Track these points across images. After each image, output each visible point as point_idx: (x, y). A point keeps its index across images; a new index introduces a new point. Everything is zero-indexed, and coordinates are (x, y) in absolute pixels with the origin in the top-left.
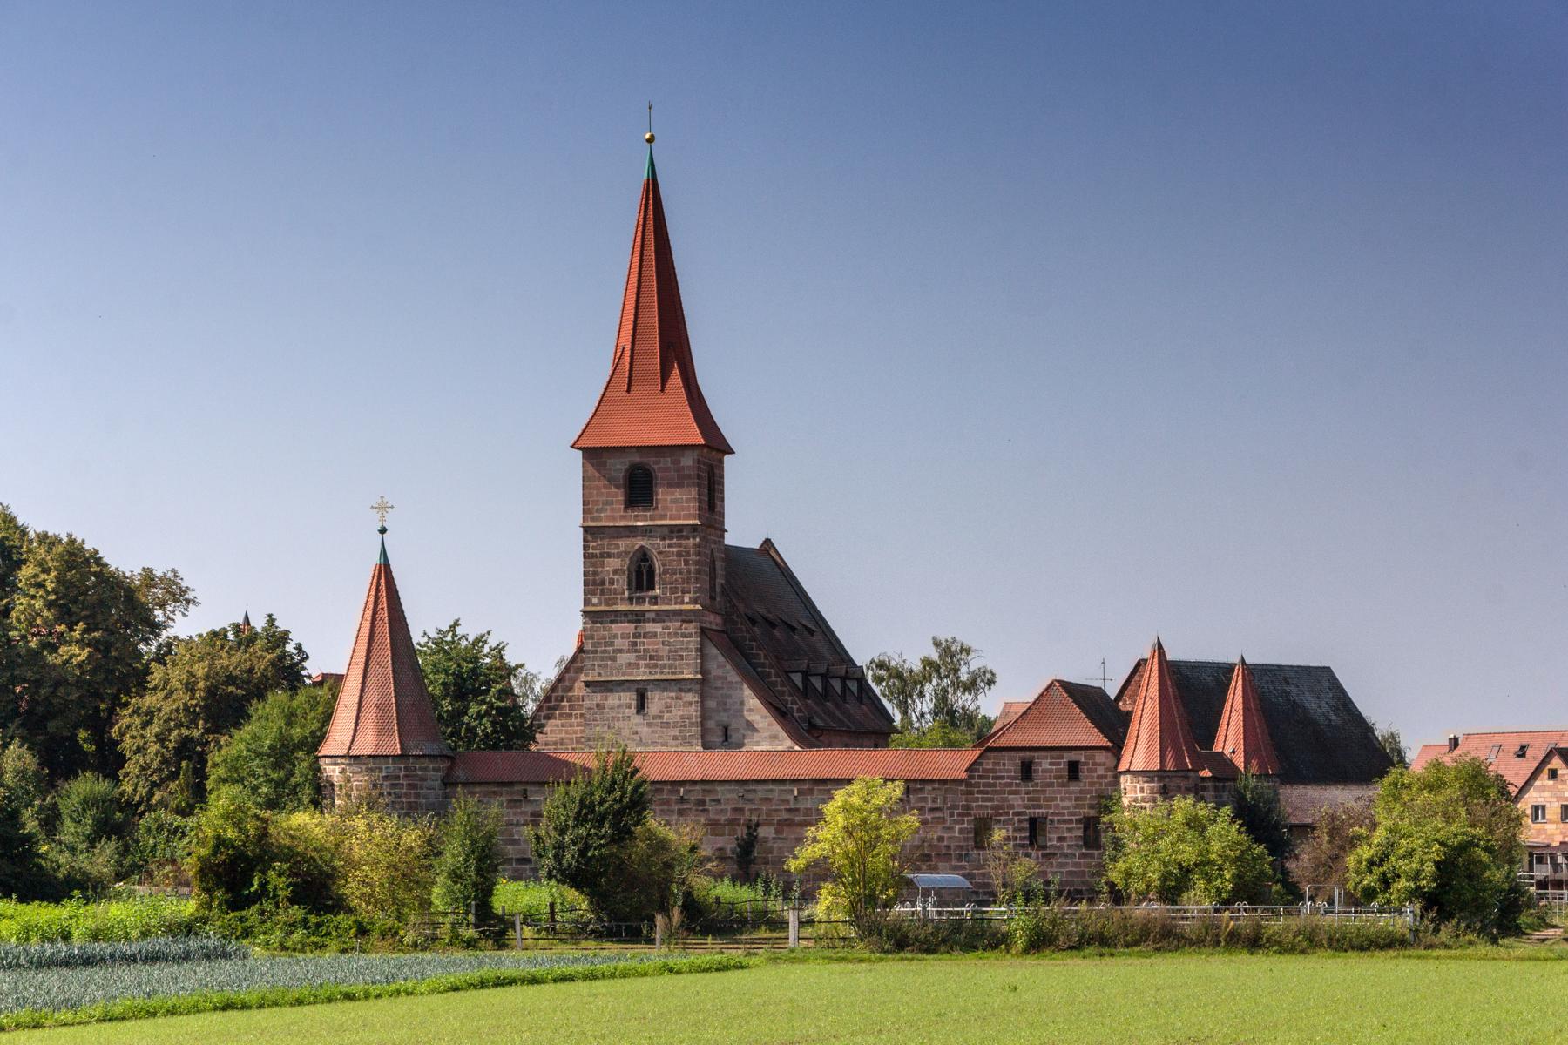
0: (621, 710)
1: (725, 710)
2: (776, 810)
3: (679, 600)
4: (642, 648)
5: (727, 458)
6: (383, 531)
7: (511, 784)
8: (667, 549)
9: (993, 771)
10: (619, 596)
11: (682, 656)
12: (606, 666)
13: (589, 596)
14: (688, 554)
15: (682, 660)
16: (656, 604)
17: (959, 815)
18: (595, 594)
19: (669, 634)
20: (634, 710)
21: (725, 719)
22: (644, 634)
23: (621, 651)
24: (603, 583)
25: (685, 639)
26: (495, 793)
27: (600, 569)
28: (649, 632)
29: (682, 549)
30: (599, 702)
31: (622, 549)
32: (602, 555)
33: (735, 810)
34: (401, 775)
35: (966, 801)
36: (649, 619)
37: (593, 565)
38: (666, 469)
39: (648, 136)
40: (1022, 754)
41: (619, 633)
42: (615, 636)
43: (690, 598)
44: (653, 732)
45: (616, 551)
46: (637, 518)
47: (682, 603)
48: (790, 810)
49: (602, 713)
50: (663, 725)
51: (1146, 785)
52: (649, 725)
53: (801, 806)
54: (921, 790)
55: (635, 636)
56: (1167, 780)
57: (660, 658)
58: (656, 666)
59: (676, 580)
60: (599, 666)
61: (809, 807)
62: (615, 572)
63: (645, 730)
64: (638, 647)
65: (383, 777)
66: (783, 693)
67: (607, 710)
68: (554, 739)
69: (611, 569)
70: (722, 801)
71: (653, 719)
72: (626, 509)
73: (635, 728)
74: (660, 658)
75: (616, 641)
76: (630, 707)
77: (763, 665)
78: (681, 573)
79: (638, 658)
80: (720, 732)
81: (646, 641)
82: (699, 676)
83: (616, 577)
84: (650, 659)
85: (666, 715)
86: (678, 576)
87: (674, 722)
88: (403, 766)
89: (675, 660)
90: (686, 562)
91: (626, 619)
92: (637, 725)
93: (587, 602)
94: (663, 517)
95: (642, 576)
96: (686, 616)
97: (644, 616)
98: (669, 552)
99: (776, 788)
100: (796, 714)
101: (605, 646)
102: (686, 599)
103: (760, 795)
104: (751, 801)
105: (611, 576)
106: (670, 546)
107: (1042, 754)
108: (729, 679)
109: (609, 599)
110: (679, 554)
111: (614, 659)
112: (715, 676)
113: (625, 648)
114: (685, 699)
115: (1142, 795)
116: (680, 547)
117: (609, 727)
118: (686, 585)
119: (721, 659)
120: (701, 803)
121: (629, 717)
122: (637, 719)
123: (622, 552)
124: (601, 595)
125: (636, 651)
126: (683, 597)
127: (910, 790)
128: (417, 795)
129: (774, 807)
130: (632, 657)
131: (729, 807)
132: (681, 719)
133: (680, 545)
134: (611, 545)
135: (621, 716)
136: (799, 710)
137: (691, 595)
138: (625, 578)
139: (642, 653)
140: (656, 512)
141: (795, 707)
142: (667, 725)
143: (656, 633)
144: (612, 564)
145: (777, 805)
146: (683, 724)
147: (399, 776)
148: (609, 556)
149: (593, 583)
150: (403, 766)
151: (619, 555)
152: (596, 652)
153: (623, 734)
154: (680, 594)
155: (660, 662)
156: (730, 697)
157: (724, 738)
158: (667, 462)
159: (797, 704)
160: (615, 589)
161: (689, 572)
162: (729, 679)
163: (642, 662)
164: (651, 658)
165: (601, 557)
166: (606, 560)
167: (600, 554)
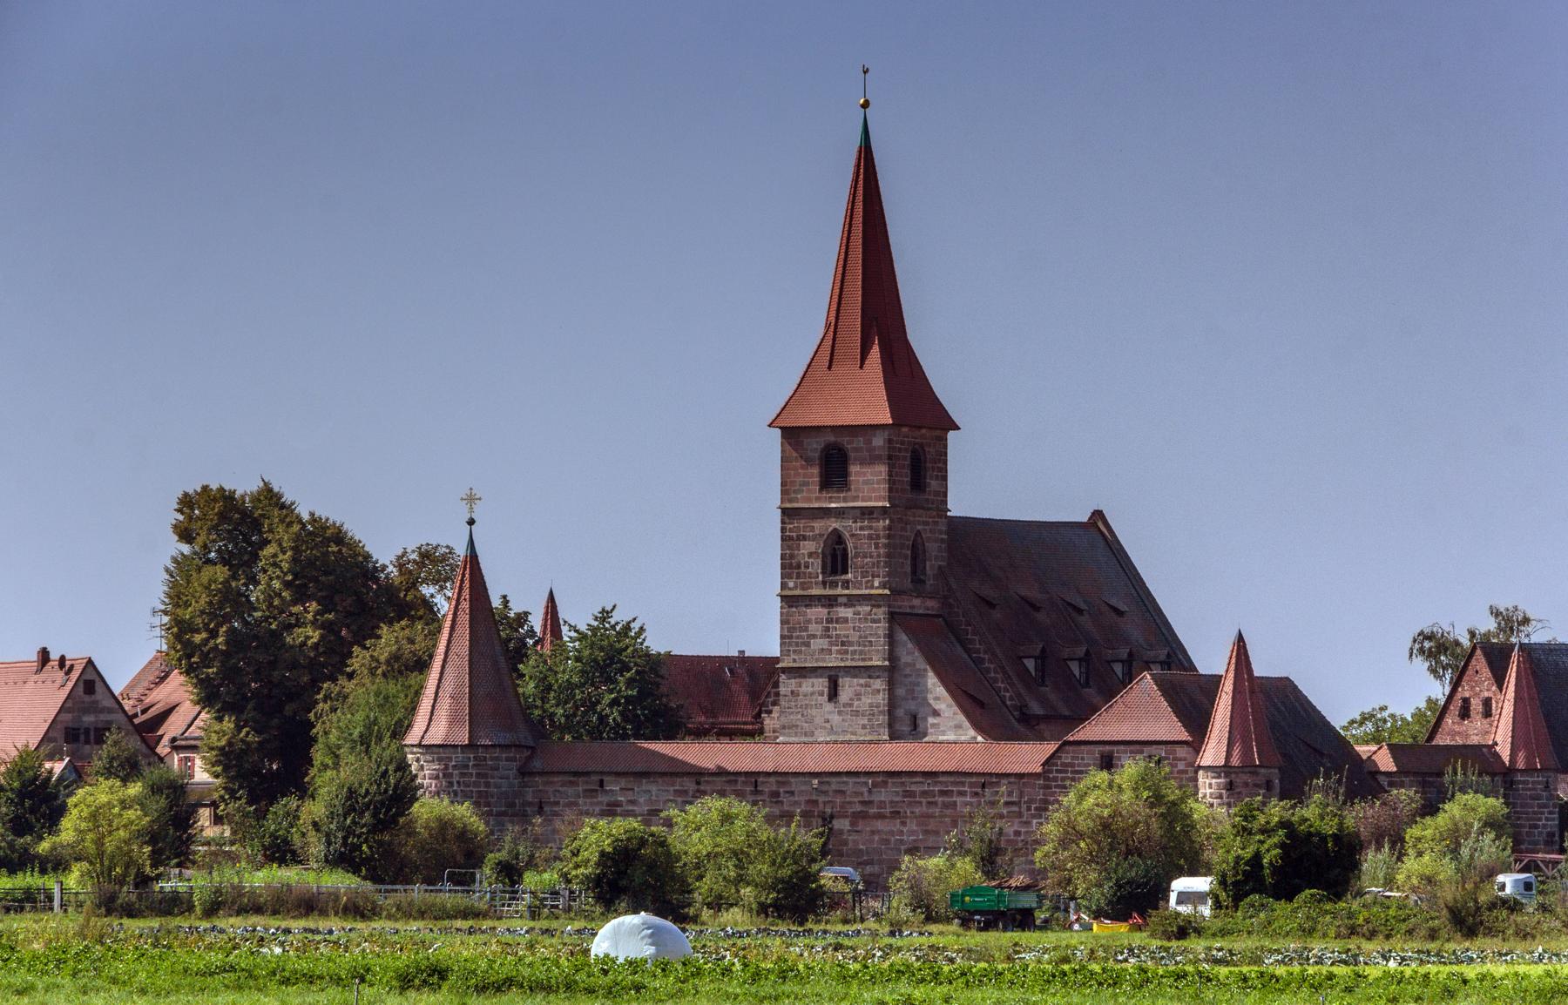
1: (913, 699)
2: (850, 803)
3: (869, 585)
5: (951, 435)
6: (471, 522)
7: (587, 774)
9: (1072, 765)
10: (813, 580)
11: (870, 642)
12: (801, 652)
13: (786, 580)
14: (878, 537)
15: (872, 646)
16: (848, 588)
17: (1036, 809)
18: (792, 578)
19: (860, 619)
20: (826, 697)
21: (913, 707)
23: (814, 636)
24: (799, 566)
25: (874, 625)
26: (571, 783)
27: (796, 552)
28: (841, 618)
31: (817, 532)
32: (798, 538)
33: (808, 802)
34: (471, 764)
35: (1044, 795)
37: (790, 548)
38: (856, 450)
39: (862, 101)
40: (1101, 748)
41: (813, 618)
42: (809, 621)
43: (880, 583)
45: (811, 533)
46: (831, 500)
47: (872, 587)
48: (863, 803)
51: (1214, 781)
52: (840, 713)
53: (875, 798)
54: (998, 784)
55: (829, 621)
56: (1233, 776)
57: (851, 643)
58: (846, 652)
60: (795, 651)
61: (883, 799)
62: (810, 555)
63: (836, 719)
65: (453, 766)
66: (996, 680)
67: (801, 697)
70: (796, 792)
71: (844, 707)
72: (821, 490)
74: (851, 643)
77: (978, 651)
78: (871, 557)
79: (831, 644)
80: (907, 720)
81: (838, 626)
82: (887, 663)
84: (842, 646)
85: (856, 703)
86: (869, 559)
88: (472, 756)
89: (865, 646)
90: (877, 547)
92: (830, 713)
93: (784, 586)
94: (855, 499)
95: (836, 559)
96: (876, 601)
97: (836, 600)
99: (851, 780)
100: (1008, 703)
101: (800, 632)
102: (876, 584)
103: (834, 787)
104: (825, 793)
105: (806, 559)
106: (861, 528)
107: (1122, 748)
108: (918, 666)
109: (805, 583)
110: (870, 537)
111: (808, 645)
113: (819, 633)
115: (1210, 790)
116: (871, 529)
117: (802, 715)
118: (875, 569)
119: (910, 645)
120: (775, 794)
122: (829, 707)
124: (797, 578)
125: (829, 637)
126: (873, 582)
127: (758, 784)
128: (487, 785)
129: (848, 799)
131: (803, 799)
135: (813, 703)
136: (1011, 699)
137: (881, 579)
138: (820, 561)
139: (834, 639)
140: (849, 494)
141: (1008, 695)
142: (856, 713)
143: (847, 618)
144: (808, 547)
145: (850, 797)
147: (468, 765)
148: (804, 538)
149: (789, 566)
150: (472, 756)
151: (814, 539)
154: (870, 578)
155: (851, 648)
158: (859, 442)
159: (1008, 691)
160: (810, 573)
161: (879, 556)
162: (918, 666)
163: (834, 648)
164: (843, 644)
166: (801, 543)
167: (797, 536)
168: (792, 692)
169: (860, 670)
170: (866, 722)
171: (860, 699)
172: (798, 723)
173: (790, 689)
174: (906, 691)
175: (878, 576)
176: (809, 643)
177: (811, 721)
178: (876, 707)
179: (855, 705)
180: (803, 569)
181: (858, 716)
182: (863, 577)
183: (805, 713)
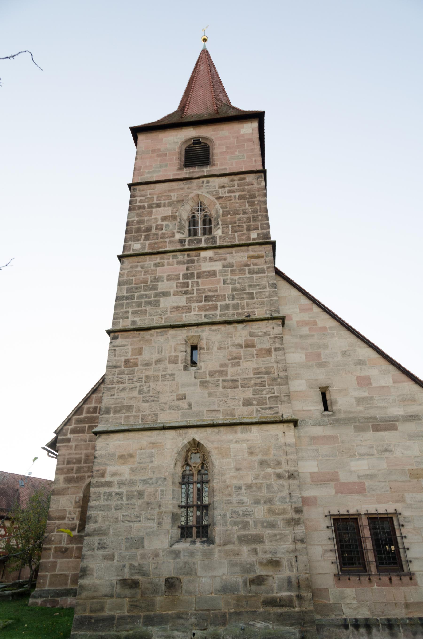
0: (161, 366)
1: (321, 365)
4: (195, 288)
8: (227, 194)
10: (167, 240)
13: (130, 243)
15: (253, 298)
18: (139, 240)
20: (181, 365)
22: (198, 273)
23: (165, 294)
24: (149, 229)
25: (254, 276)
27: (146, 218)
28: (204, 272)
29: (245, 193)
30: (129, 357)
31: (175, 199)
32: (150, 207)
36: (205, 258)
37: (138, 215)
42: (157, 279)
43: (258, 235)
44: (210, 395)
49: (133, 372)
50: (226, 384)
52: (204, 384)
59: (239, 219)
62: (164, 219)
64: (190, 288)
67: (140, 367)
68: (78, 456)
69: (159, 217)
71: (210, 375)
73: (182, 391)
75: (159, 283)
76: (174, 361)
78: (244, 213)
79: (189, 300)
81: (199, 280)
83: (164, 223)
85: (231, 370)
86: (241, 216)
87: (244, 379)
89: (242, 299)
91: (175, 261)
92: (184, 385)
97: (199, 255)
98: (231, 196)
101: (145, 290)
105: (159, 222)
108: (320, 324)
111: (156, 303)
112: (298, 322)
114: (258, 347)
116: (244, 191)
117: (140, 392)
118: (252, 223)
121: (173, 375)
123: (174, 201)
125: (186, 293)
126: (249, 234)
130: (182, 301)
132: (255, 374)
134: (162, 197)
137: (260, 231)
146: (258, 381)
151: (170, 204)
152: (132, 298)
153: (162, 401)
154: (245, 231)
155: (219, 304)
156: (326, 346)
157: (322, 407)
162: (320, 324)
164: (207, 299)
165: (148, 208)
166: (154, 210)
168: (127, 362)
169: (236, 328)
170: (249, 394)
171: (238, 364)
172: (132, 403)
173: (123, 359)
174: (307, 356)
175: (256, 229)
176: (158, 301)
177: (156, 400)
178: (267, 373)
179: (229, 372)
180: (154, 231)
181: (237, 387)
182: (234, 231)
183: (145, 389)
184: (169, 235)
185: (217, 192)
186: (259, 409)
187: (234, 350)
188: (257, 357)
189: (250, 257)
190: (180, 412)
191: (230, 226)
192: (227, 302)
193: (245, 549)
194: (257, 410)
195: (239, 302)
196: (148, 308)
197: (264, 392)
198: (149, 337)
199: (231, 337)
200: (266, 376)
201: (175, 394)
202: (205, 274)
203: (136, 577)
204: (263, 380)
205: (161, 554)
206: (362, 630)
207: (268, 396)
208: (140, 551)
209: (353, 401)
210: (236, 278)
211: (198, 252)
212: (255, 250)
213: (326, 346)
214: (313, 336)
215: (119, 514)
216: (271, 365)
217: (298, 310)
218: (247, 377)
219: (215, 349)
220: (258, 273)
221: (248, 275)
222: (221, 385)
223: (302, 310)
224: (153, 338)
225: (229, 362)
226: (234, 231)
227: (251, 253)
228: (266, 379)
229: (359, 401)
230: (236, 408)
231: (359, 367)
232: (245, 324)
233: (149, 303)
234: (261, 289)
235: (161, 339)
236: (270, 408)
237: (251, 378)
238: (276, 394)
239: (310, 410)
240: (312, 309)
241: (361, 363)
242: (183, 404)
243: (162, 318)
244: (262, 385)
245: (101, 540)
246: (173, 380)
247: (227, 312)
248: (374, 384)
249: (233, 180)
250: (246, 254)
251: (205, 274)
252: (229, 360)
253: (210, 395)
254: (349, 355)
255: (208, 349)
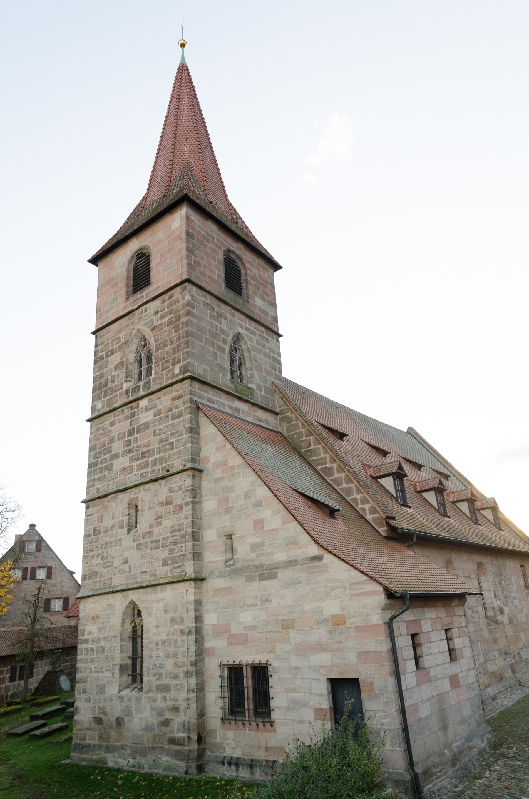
8: (160, 322)
21: (227, 524)
57: (151, 452)
58: (147, 465)
63: (134, 556)
66: (349, 492)
74: (151, 452)
79: (132, 460)
80: (221, 544)
85: (156, 530)
96: (177, 391)
100: (369, 517)
110: (170, 322)
121: (120, 540)
122: (128, 541)
133: (170, 312)
136: (373, 511)
141: (367, 506)
142: (156, 544)
153: (114, 566)
154: (171, 367)
159: (368, 502)
161: (179, 339)
163: (135, 464)
164: (144, 455)
170: (166, 554)
178: (179, 530)
184: (119, 387)
185: (152, 321)
186: (172, 569)
187: (158, 508)
188: (173, 515)
189: (174, 399)
190: (124, 575)
191: (160, 363)
192: (156, 456)
193: (159, 696)
194: (171, 570)
195: (163, 454)
196: (106, 473)
197: (176, 551)
198: (106, 504)
199: (157, 495)
200: (178, 533)
201: (121, 558)
202: (142, 427)
203: (101, 716)
204: (176, 538)
205: (114, 698)
206: (233, 767)
207: (178, 554)
208: (103, 696)
209: (248, 548)
210: (162, 427)
211: (137, 402)
212: (177, 389)
213: (231, 489)
214: (223, 478)
215: (93, 666)
216: (182, 521)
217: (214, 450)
218: (166, 536)
219: (146, 510)
220: (178, 417)
221: (171, 422)
222: (149, 547)
223: (218, 449)
224: (109, 504)
225: (155, 521)
226: (163, 369)
227: (174, 394)
228: (177, 537)
229: (254, 547)
230: (158, 568)
231: (256, 509)
232: (166, 479)
233: (107, 468)
234: (179, 436)
235: (114, 504)
236: (180, 566)
237: (168, 537)
238: (184, 552)
239: (217, 561)
240: (225, 446)
241: (258, 504)
242: (126, 567)
243: (114, 482)
244: (175, 543)
245: (84, 686)
246: (121, 545)
247: (155, 467)
248: (266, 528)
249: (164, 302)
250: (169, 397)
251: (142, 427)
252: (155, 520)
253: (142, 557)
254: (250, 497)
255: (142, 510)
